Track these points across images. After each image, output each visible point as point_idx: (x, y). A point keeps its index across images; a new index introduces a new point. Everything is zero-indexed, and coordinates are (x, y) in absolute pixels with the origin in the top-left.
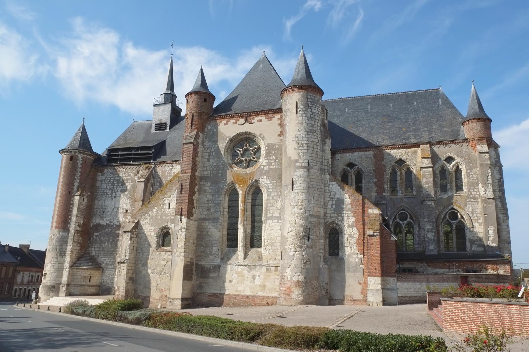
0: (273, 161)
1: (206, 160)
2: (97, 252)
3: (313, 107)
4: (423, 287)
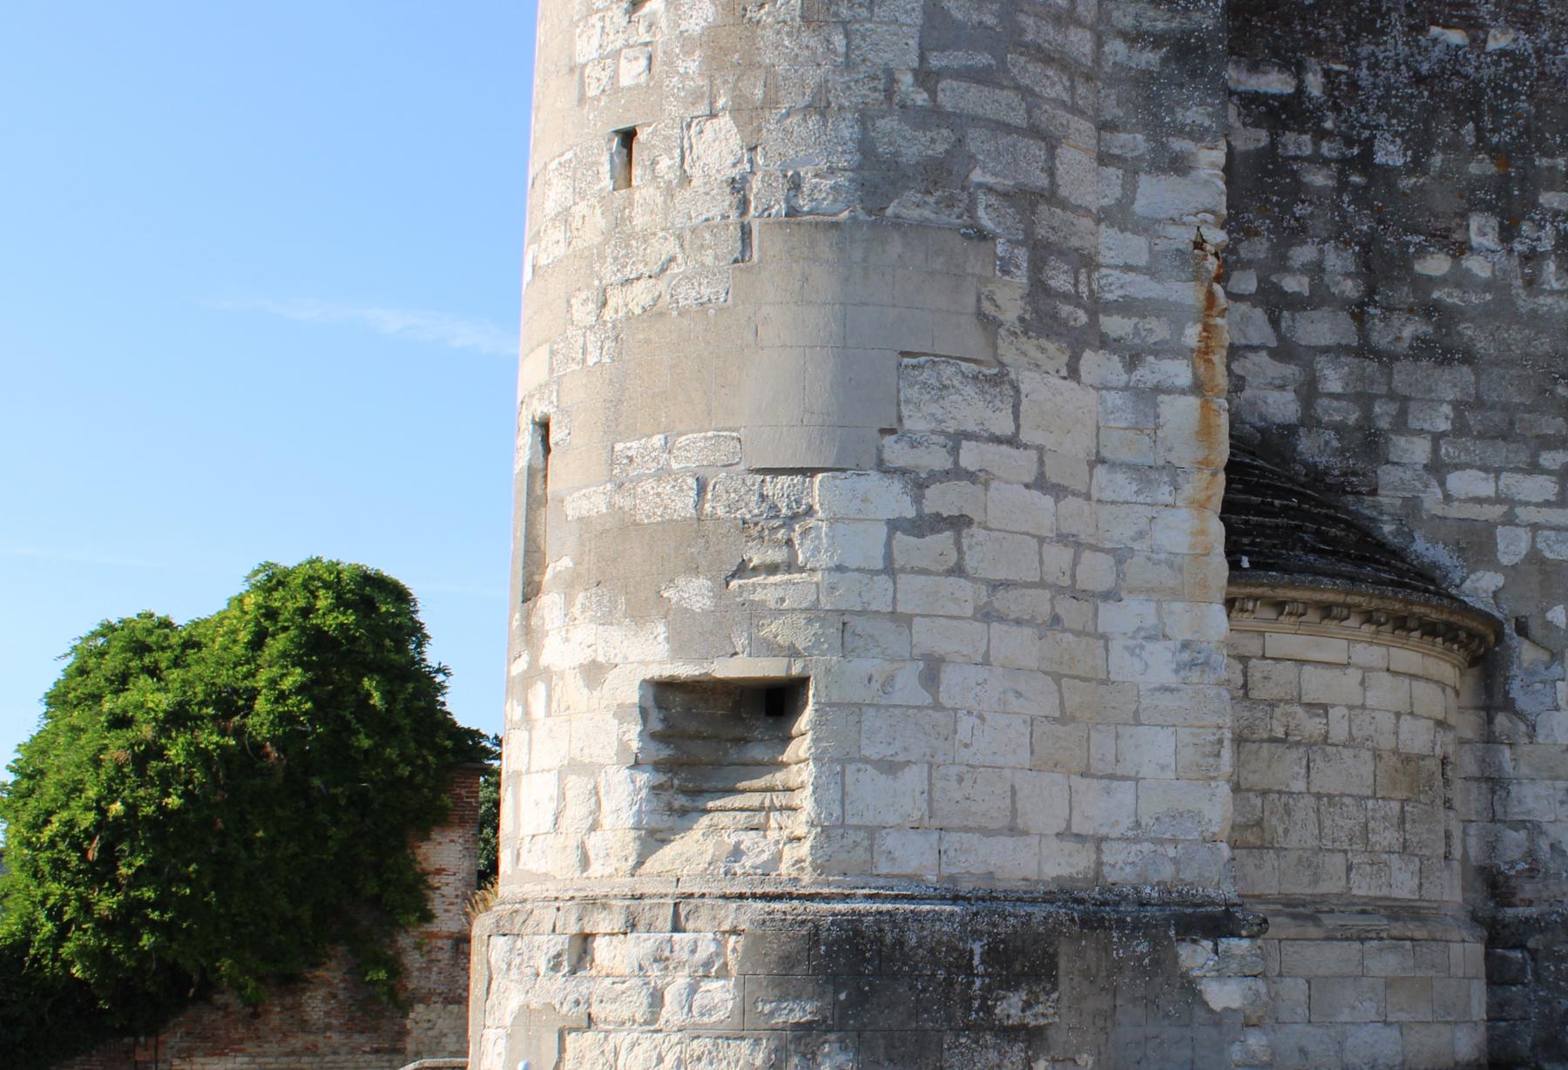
2: (1333, 379)
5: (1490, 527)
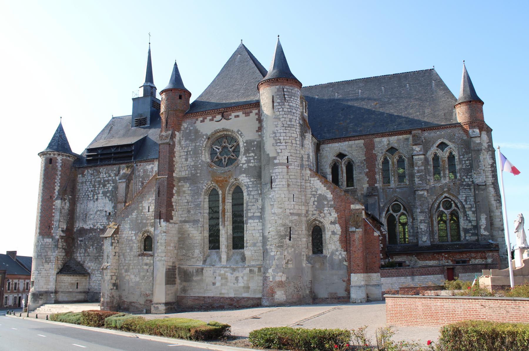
0: (252, 159)
1: (184, 160)
2: (83, 258)
3: (290, 100)
4: (408, 281)
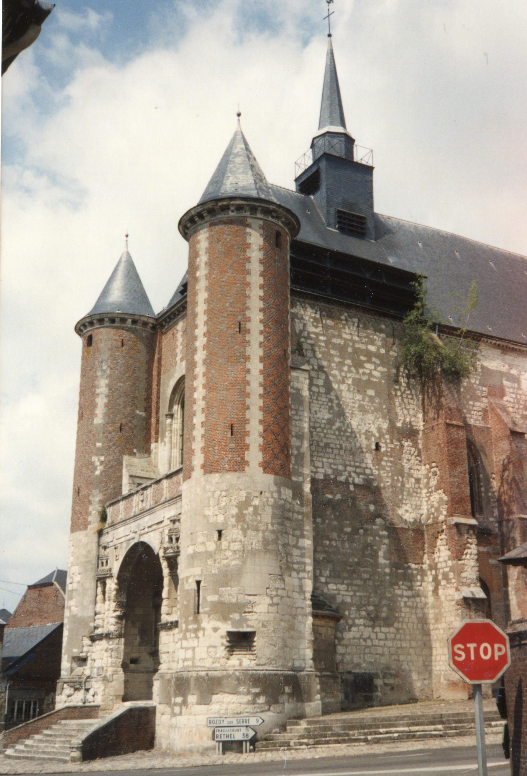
5: (335, 595)
